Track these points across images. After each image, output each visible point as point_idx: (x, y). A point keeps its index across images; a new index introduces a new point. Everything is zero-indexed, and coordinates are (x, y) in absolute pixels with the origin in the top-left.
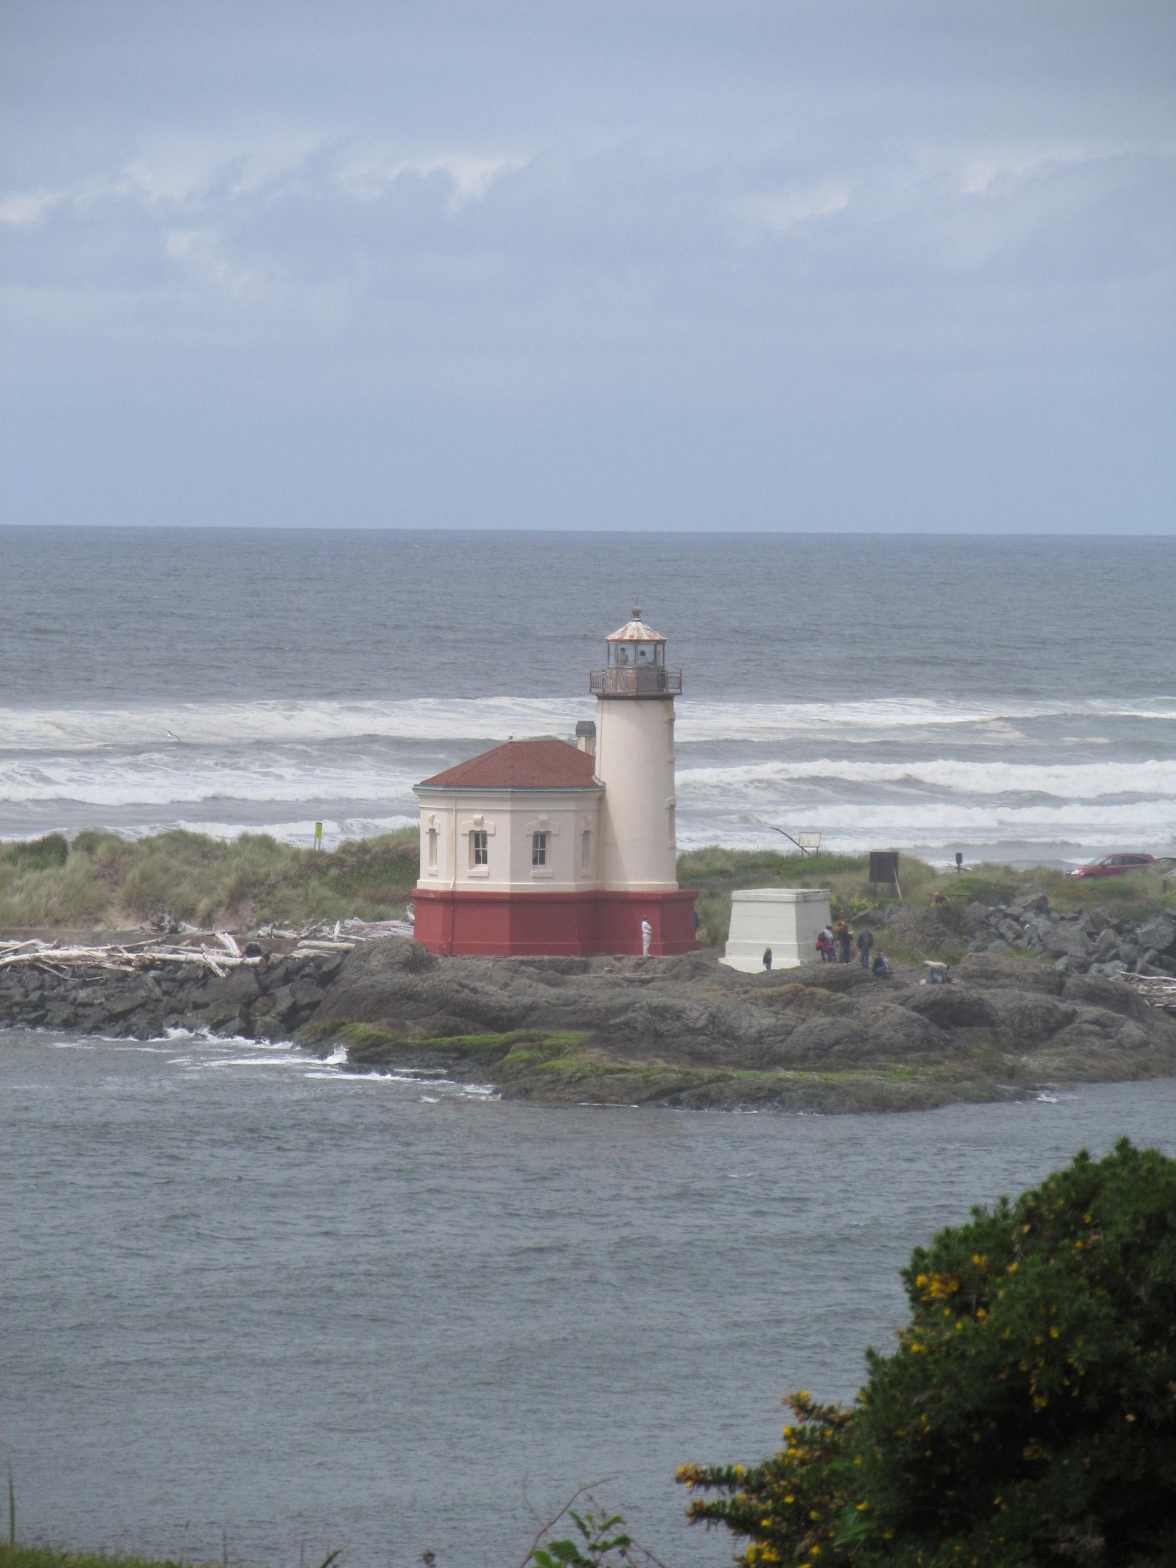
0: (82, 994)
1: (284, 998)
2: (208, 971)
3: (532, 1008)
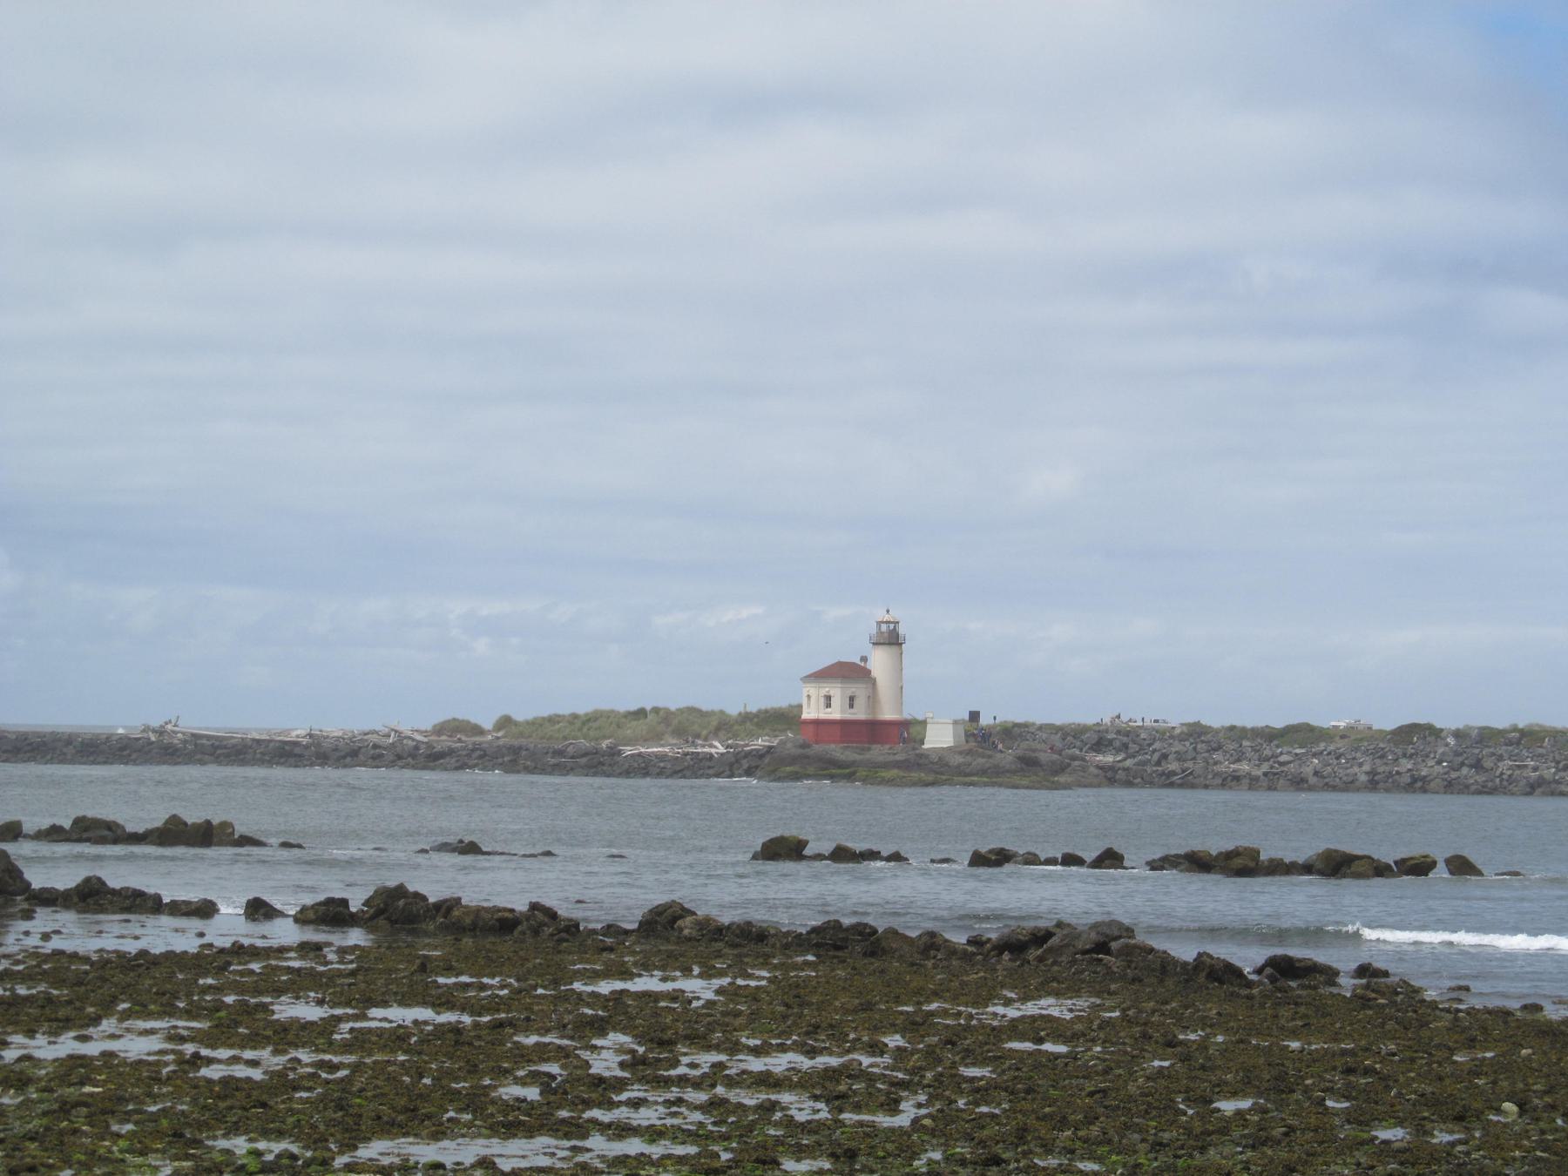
1: (745, 764)
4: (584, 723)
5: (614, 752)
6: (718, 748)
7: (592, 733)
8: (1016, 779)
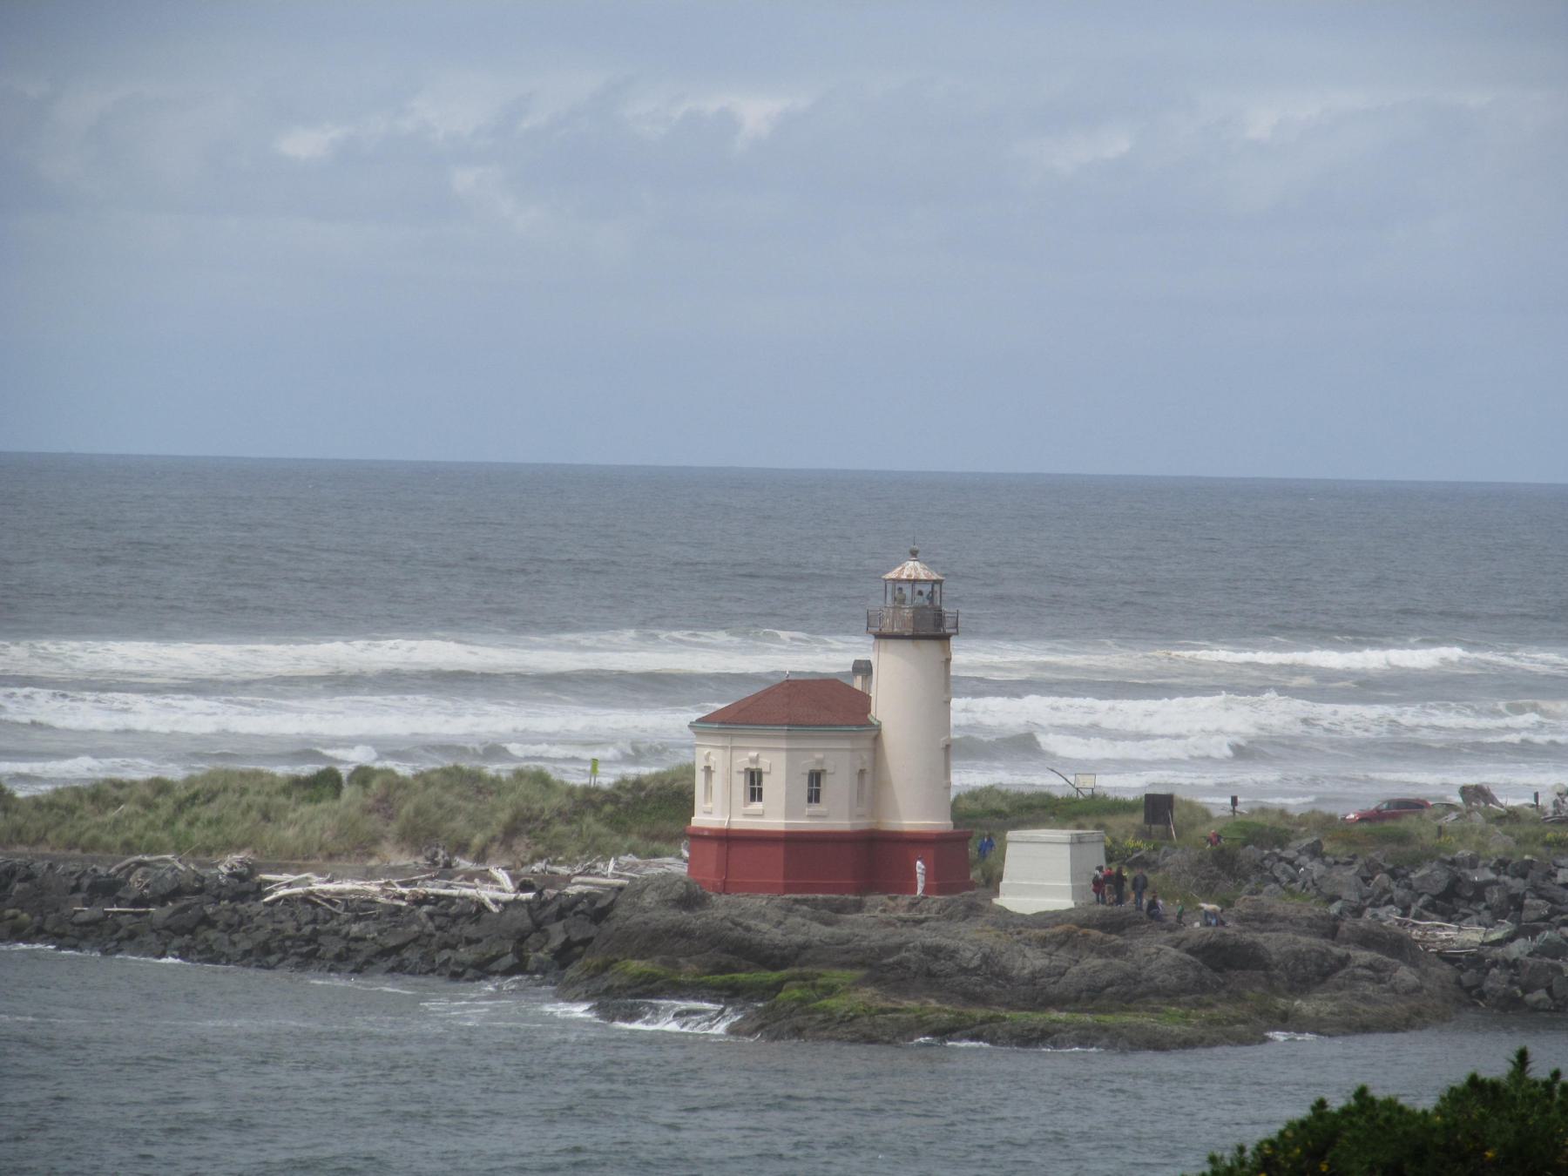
0: (355, 929)
2: (481, 907)
3: (804, 947)
4: (180, 807)
5: (246, 886)
6: (497, 887)
7: (198, 835)
8: (1170, 1022)
